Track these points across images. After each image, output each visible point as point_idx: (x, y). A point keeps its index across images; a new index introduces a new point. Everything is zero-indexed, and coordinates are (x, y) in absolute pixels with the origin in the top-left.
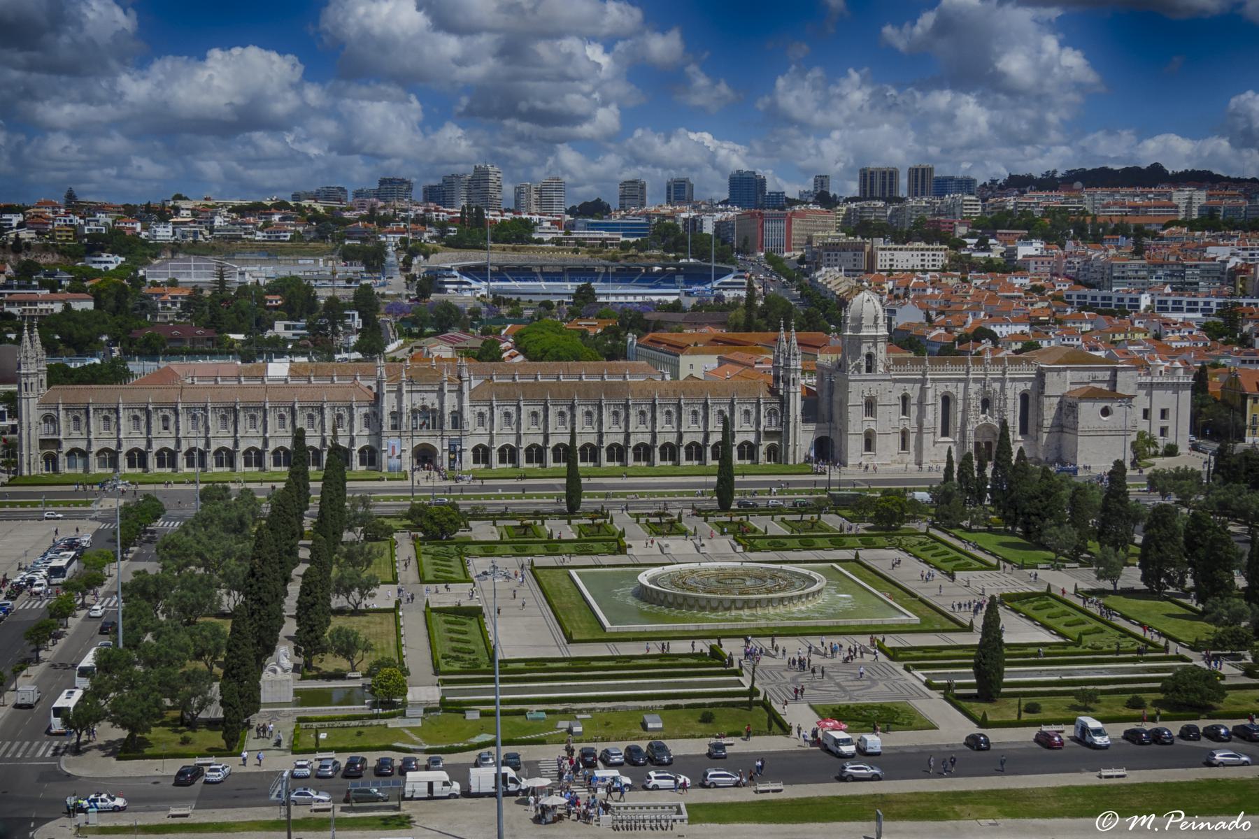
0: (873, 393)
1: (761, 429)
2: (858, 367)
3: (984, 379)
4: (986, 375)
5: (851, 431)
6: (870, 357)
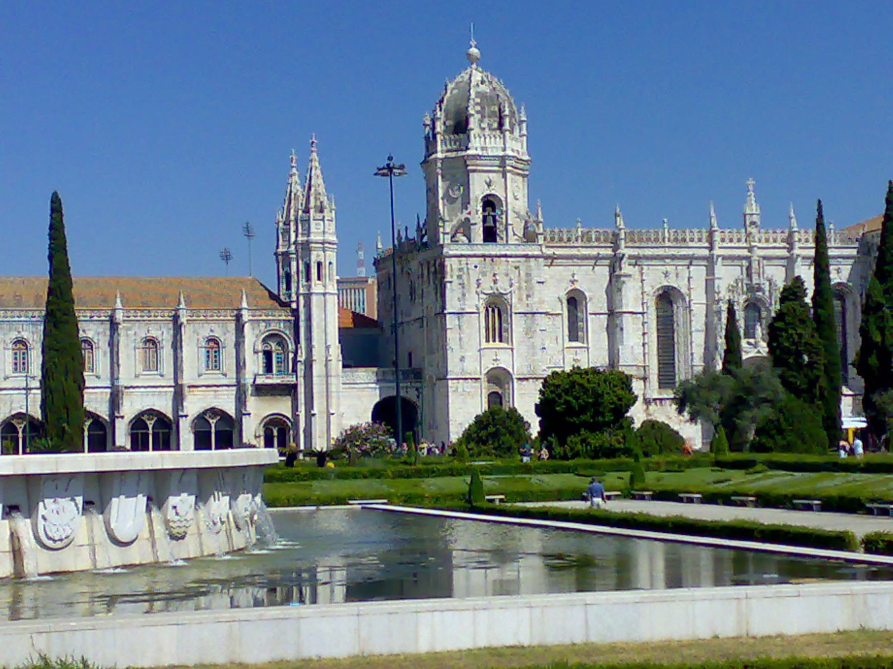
0: (503, 286)
1: (249, 380)
2: (465, 227)
3: (748, 258)
4: (750, 249)
5: (453, 367)
6: (489, 203)
